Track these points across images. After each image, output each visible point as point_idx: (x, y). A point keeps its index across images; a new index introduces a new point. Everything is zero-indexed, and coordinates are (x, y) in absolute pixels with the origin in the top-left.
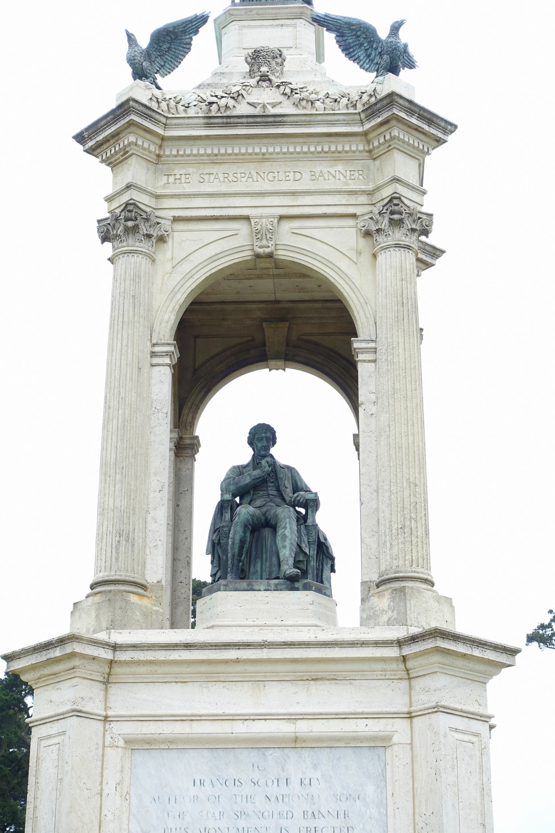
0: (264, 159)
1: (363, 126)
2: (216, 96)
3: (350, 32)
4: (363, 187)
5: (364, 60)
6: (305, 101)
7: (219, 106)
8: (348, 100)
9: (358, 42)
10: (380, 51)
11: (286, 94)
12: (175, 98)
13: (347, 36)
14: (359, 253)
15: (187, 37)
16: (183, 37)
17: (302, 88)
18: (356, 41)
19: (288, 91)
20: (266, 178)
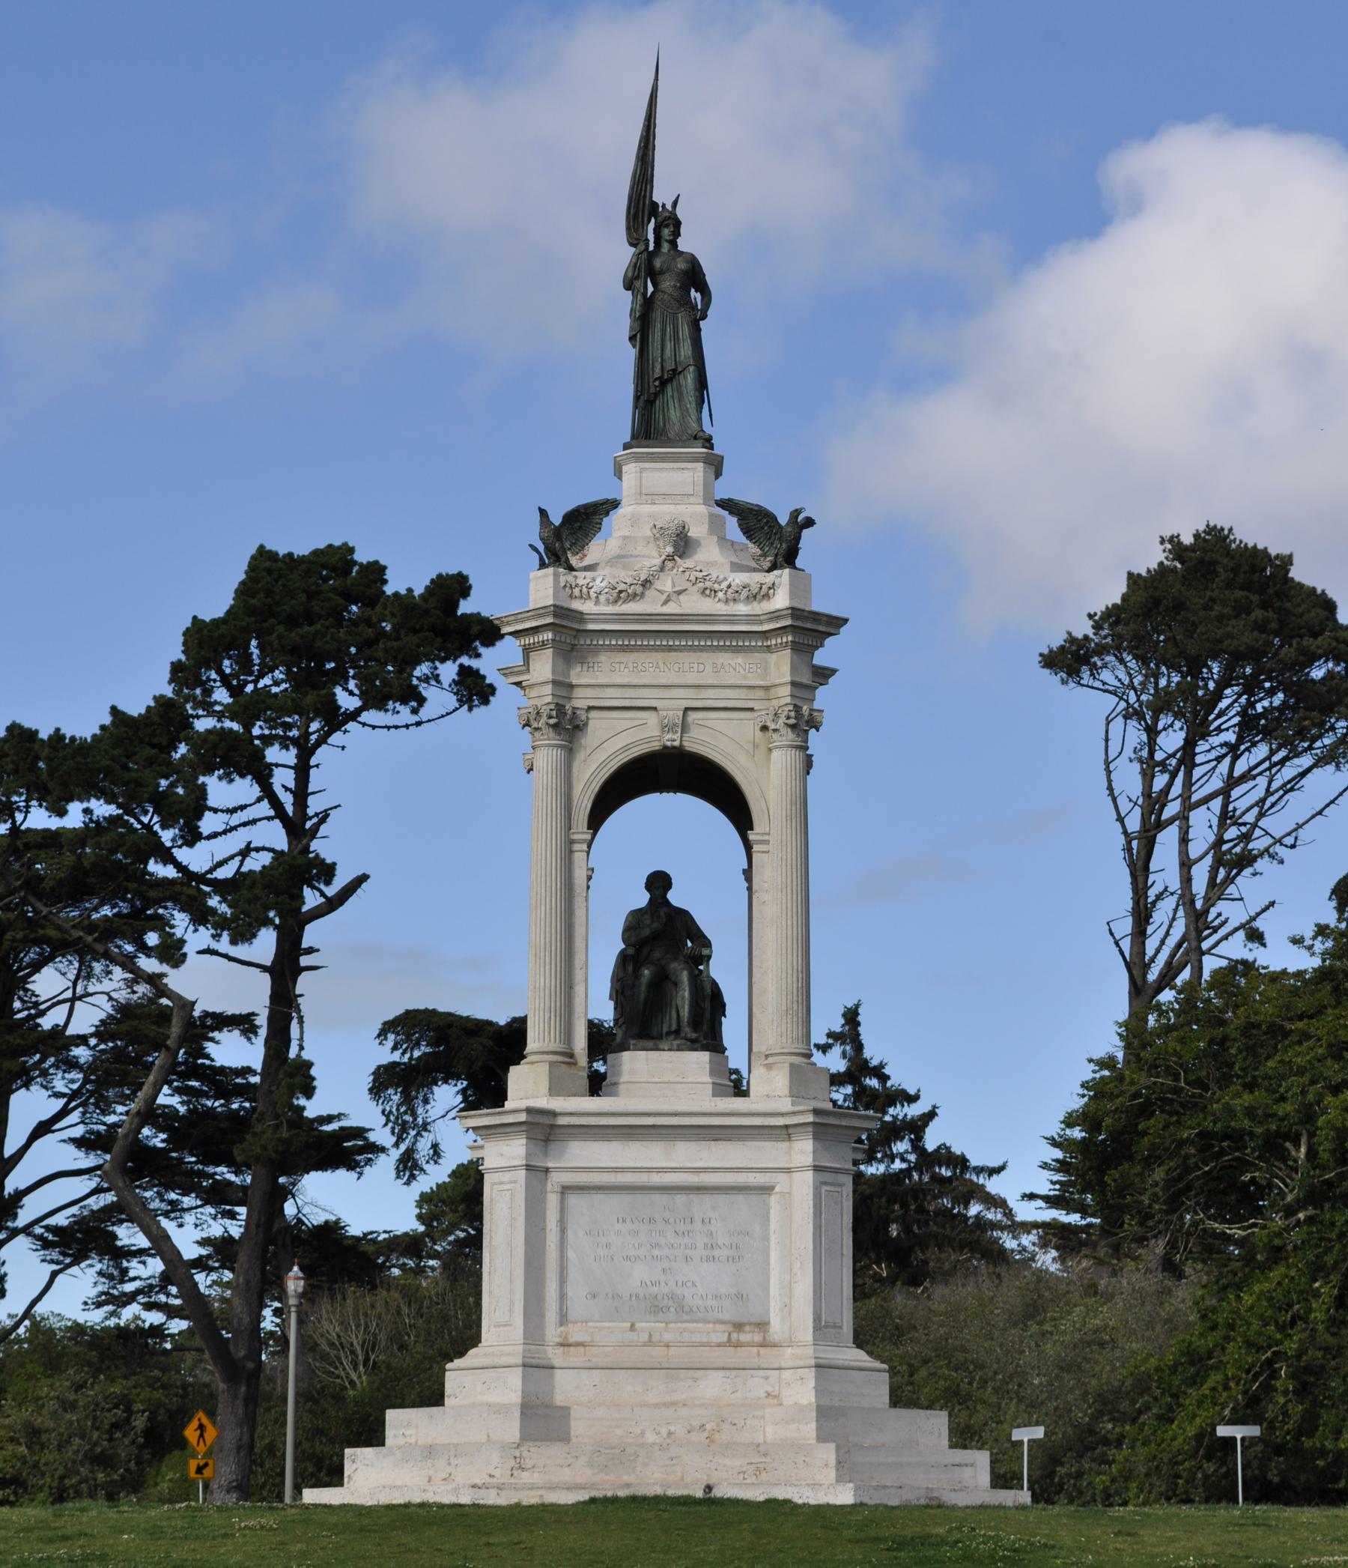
4: (762, 683)
14: (755, 746)
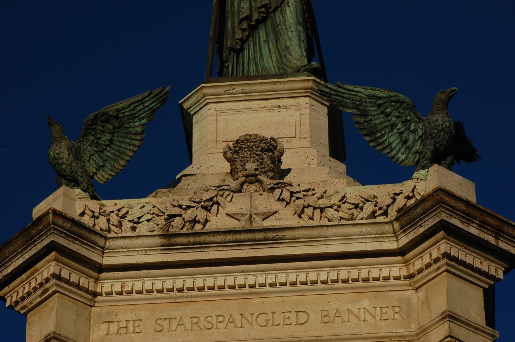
0: (252, 293)
1: (397, 240)
2: (180, 206)
3: (375, 108)
5: (398, 149)
6: (311, 209)
7: (184, 219)
8: (376, 206)
9: (387, 124)
10: (420, 134)
11: (283, 200)
12: (119, 210)
13: (371, 115)
15: (137, 124)
16: (132, 125)
17: (307, 191)
18: (385, 122)
19: (286, 195)
20: (254, 322)
